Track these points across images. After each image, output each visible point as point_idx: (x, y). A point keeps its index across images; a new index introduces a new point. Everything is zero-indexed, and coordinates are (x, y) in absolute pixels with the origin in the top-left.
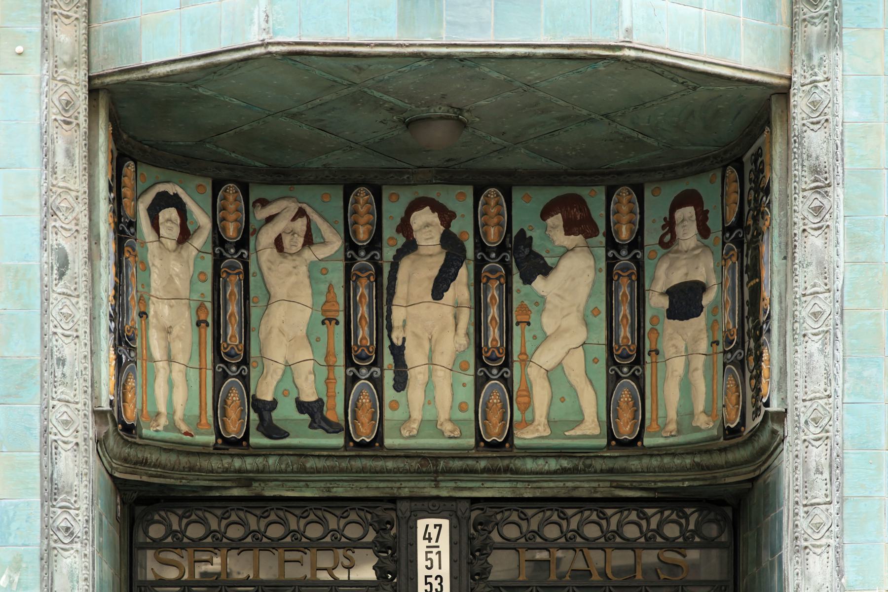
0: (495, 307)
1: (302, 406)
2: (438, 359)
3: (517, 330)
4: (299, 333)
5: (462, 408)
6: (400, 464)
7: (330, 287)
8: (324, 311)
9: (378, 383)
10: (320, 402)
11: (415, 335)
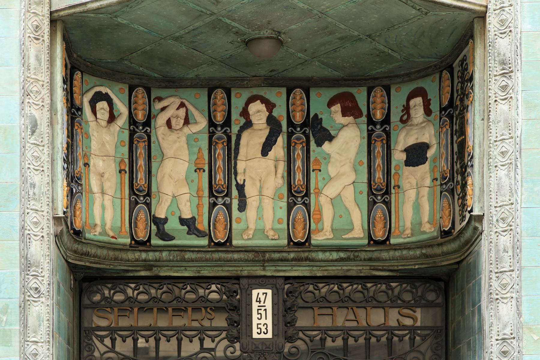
0: (300, 161)
1: (183, 221)
2: (265, 192)
3: (313, 175)
4: (181, 177)
5: (280, 221)
6: (242, 256)
7: (200, 150)
8: (196, 164)
9: (229, 207)
10: (193, 219)
11: (251, 178)
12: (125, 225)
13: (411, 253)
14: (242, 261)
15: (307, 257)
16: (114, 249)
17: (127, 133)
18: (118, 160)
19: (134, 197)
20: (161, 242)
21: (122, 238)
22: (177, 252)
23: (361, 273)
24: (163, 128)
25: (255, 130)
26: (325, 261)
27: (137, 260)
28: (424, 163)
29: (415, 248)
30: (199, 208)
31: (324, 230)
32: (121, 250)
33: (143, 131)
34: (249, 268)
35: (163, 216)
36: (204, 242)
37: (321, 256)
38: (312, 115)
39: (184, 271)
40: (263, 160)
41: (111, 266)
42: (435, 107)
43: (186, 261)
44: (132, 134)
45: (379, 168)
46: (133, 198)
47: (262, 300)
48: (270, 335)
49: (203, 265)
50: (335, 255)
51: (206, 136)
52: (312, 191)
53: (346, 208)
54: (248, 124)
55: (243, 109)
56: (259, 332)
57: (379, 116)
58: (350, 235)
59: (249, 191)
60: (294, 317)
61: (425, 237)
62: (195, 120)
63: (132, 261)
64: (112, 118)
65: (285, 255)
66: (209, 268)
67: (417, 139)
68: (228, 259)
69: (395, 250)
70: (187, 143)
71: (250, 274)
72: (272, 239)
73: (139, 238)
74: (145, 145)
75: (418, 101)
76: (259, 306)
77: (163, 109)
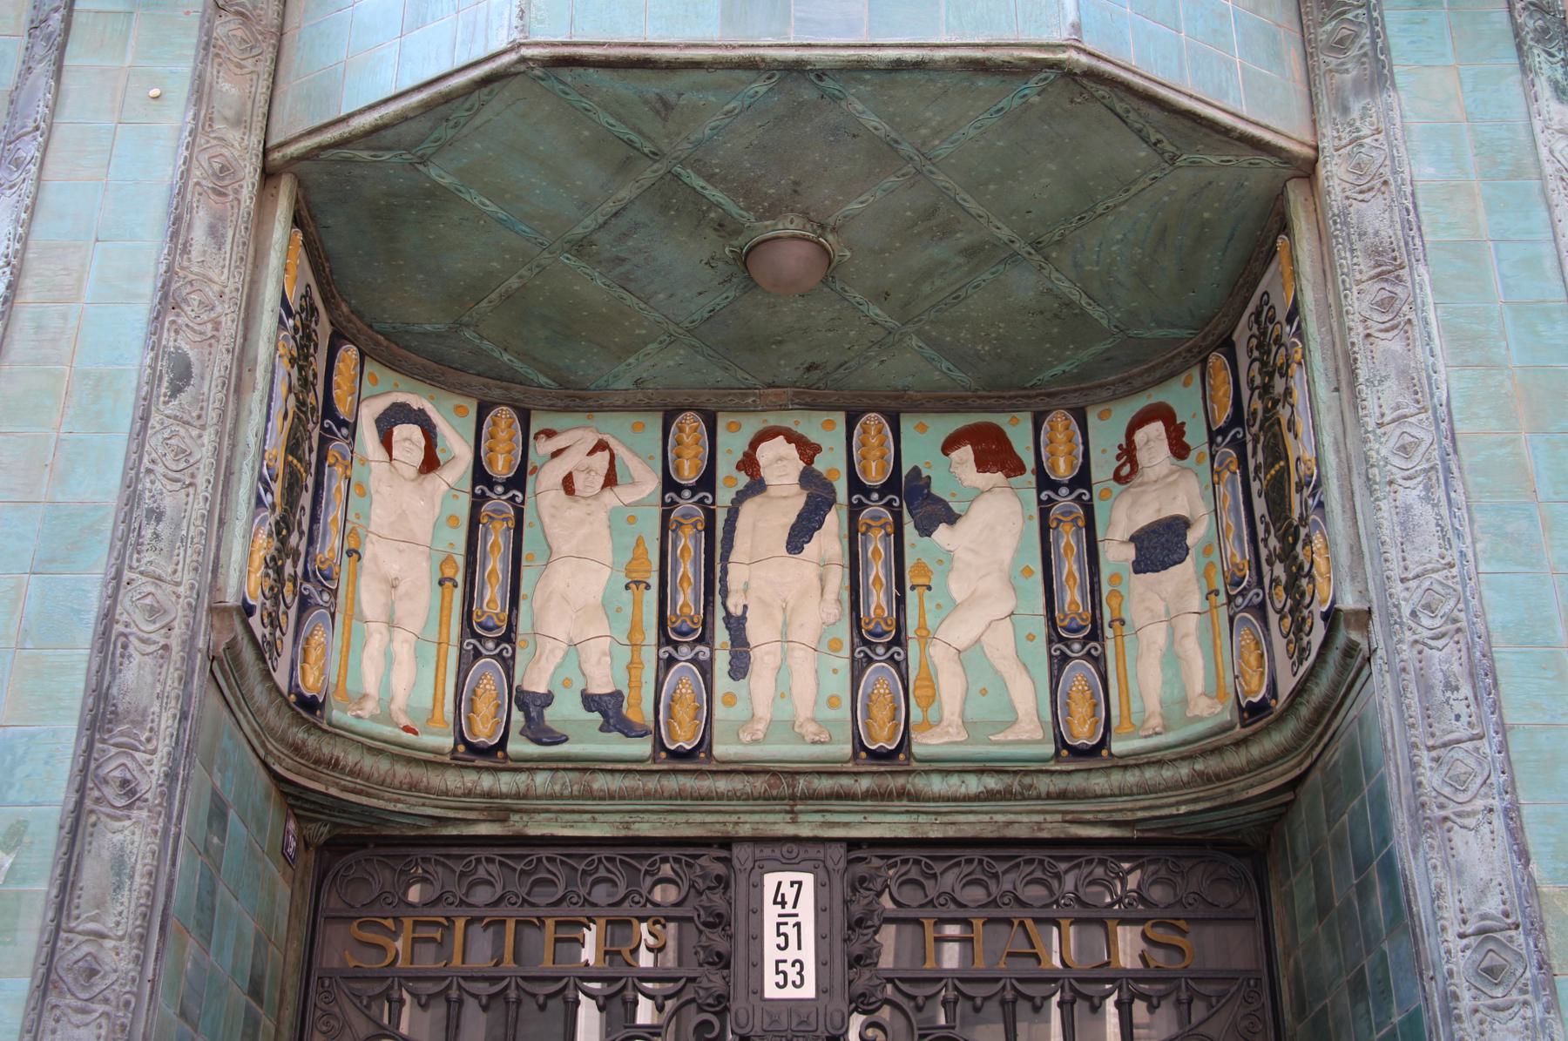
1: (590, 701)
3: (911, 597)
5: (833, 702)
7: (640, 542)
8: (628, 572)
9: (706, 669)
10: (617, 696)
12: (443, 706)
13: (1167, 773)
14: (739, 799)
15: (904, 788)
16: (410, 761)
17: (465, 501)
18: (440, 557)
19: (472, 641)
21: (433, 734)
22: (572, 775)
23: (1041, 830)
24: (553, 493)
25: (772, 498)
26: (948, 799)
27: (469, 793)
28: (1182, 561)
29: (1175, 760)
30: (633, 671)
31: (945, 723)
32: (427, 763)
33: (504, 497)
34: (756, 818)
35: (542, 689)
37: (937, 785)
38: (905, 470)
39: (588, 825)
40: (792, 560)
41: (400, 805)
42: (1196, 436)
43: (594, 799)
44: (477, 502)
45: (1071, 582)
46: (468, 644)
47: (790, 899)
48: (808, 991)
49: (638, 807)
50: (973, 784)
51: (657, 512)
52: (911, 633)
53: (997, 672)
54: (757, 486)
55: (745, 454)
56: (782, 983)
57: (1063, 470)
58: (1010, 736)
59: (756, 631)
60: (871, 944)
61: (1200, 728)
62: (631, 476)
63: (455, 796)
64: (430, 463)
65: (846, 782)
66: (654, 817)
67: (1159, 510)
68: (703, 792)
69: (1125, 767)
70: (610, 527)
71: (758, 834)
72: (814, 743)
73: (475, 735)
74: (509, 529)
75: (1156, 429)
76: (780, 916)
77: (556, 454)
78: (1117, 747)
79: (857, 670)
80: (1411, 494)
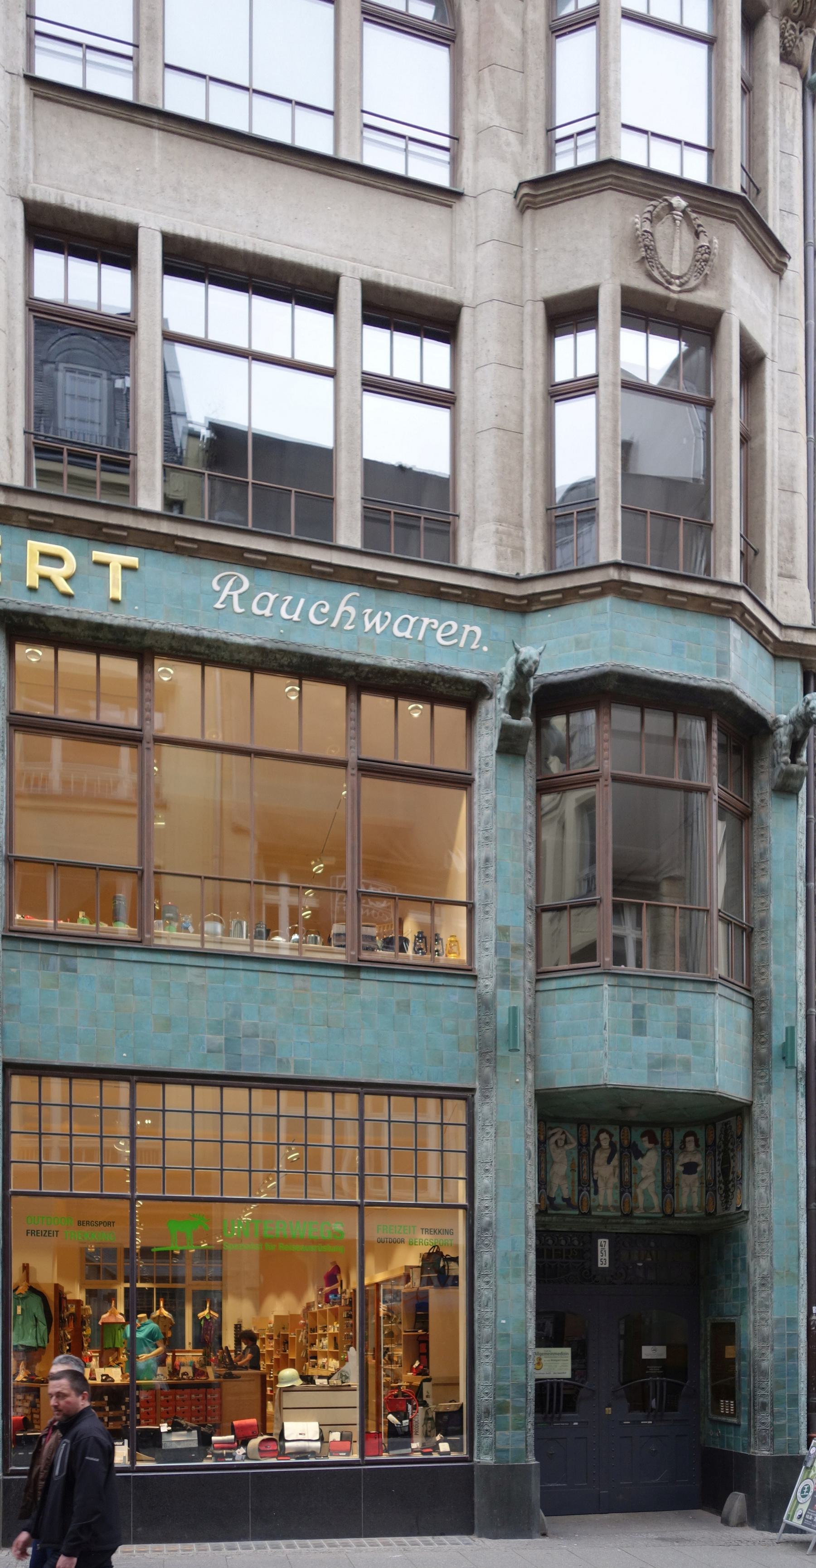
1: (564, 1199)
3: (633, 1176)
7: (573, 1159)
9: (589, 1192)
20: (553, 1212)
36: (577, 1212)
48: (607, 1265)
50: (644, 1221)
54: (599, 1146)
59: (600, 1184)
75: (692, 1138)
78: (676, 1215)
79: (621, 1194)
80: (762, 1190)
